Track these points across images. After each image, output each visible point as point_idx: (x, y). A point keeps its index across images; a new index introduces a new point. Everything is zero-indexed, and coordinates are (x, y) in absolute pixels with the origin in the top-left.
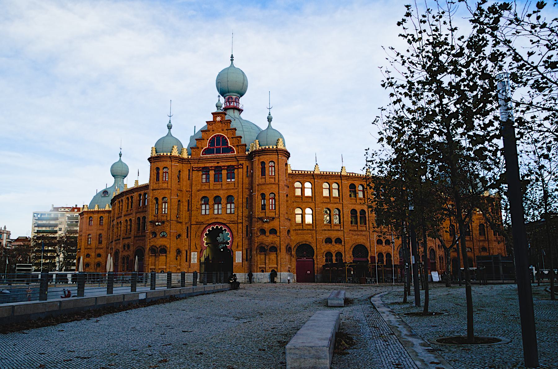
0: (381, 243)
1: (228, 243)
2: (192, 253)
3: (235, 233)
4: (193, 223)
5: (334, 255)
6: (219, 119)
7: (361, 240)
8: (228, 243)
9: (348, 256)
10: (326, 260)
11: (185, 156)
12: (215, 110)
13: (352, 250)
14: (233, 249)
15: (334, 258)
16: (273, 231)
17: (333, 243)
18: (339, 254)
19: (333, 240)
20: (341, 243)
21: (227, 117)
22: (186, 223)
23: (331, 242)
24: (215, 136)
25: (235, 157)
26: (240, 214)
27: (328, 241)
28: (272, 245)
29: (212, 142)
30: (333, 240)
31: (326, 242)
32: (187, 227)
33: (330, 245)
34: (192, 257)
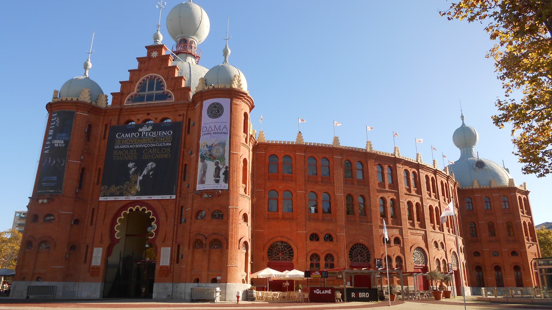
1: (152, 235)
2: (95, 249)
3: (162, 218)
6: (155, 54)
9: (342, 259)
12: (151, 43)
14: (158, 242)
15: (322, 262)
17: (322, 239)
20: (331, 240)
24: (148, 78)
25: (173, 105)
27: (314, 237)
28: (215, 237)
29: (142, 88)
31: (311, 240)
32: (94, 209)
33: (316, 243)
34: (94, 255)
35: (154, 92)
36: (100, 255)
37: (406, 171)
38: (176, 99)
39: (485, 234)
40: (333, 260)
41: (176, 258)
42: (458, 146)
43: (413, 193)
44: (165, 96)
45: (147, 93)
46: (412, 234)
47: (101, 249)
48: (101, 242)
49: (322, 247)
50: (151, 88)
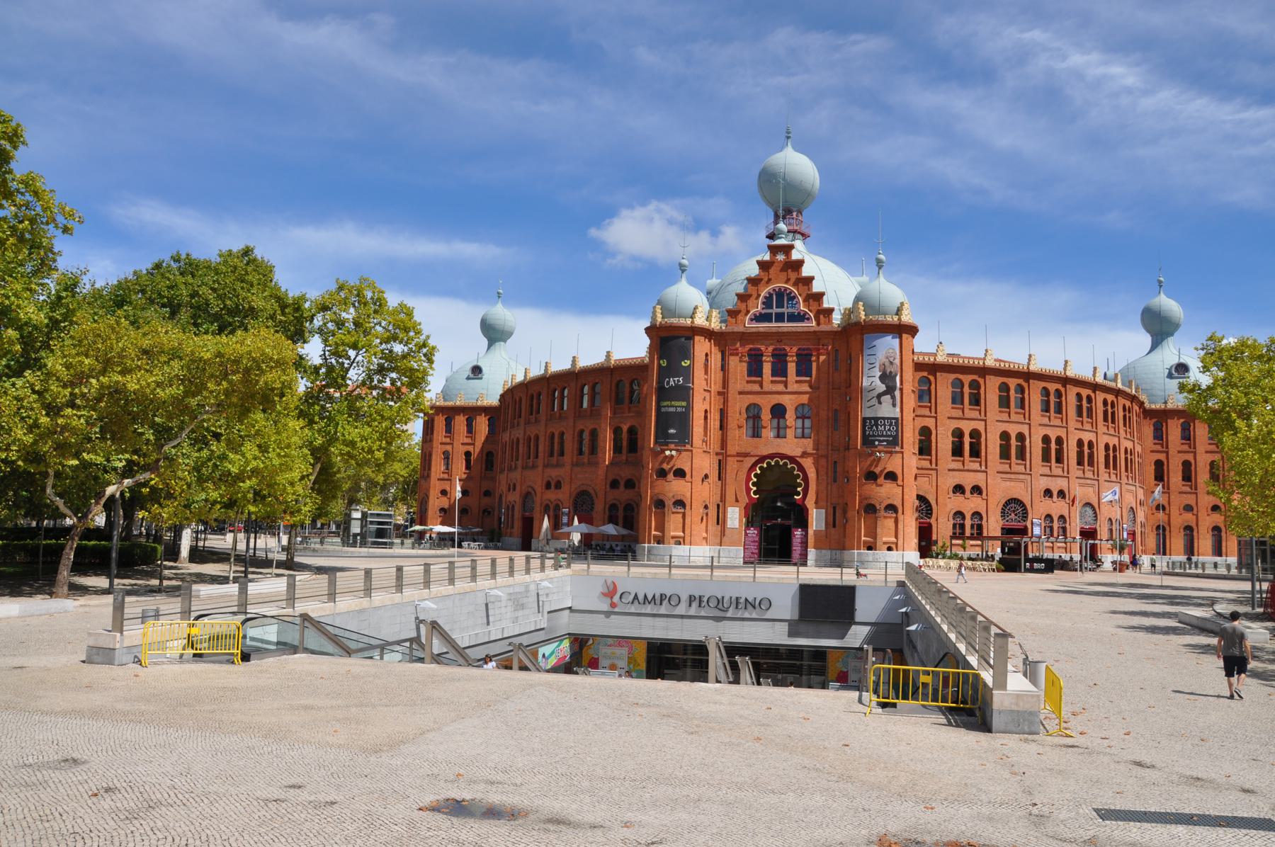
0: (1051, 496)
2: (730, 510)
4: (732, 449)
5: (968, 516)
7: (1018, 491)
8: (798, 494)
10: (954, 525)
11: (715, 325)
13: (1001, 506)
15: (968, 523)
16: (891, 476)
17: (968, 494)
18: (977, 514)
19: (968, 489)
20: (980, 493)
21: (795, 255)
22: (717, 454)
23: (963, 492)
26: (823, 440)
27: (959, 489)
28: (889, 502)
29: (768, 303)
30: (968, 489)
34: (729, 515)
35: (784, 310)
36: (737, 515)
37: (1079, 395)
38: (818, 324)
39: (1176, 477)
40: (981, 518)
41: (832, 522)
42: (1148, 331)
43: (1088, 427)
44: (801, 317)
45: (775, 310)
46: (1081, 485)
47: (737, 509)
48: (737, 501)
49: (970, 504)
50: (780, 305)
